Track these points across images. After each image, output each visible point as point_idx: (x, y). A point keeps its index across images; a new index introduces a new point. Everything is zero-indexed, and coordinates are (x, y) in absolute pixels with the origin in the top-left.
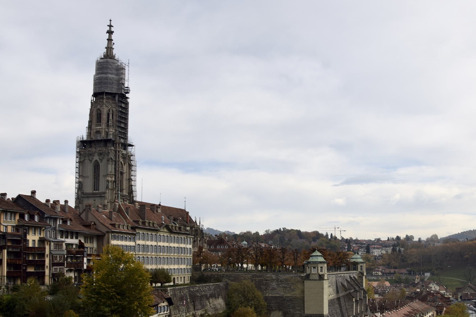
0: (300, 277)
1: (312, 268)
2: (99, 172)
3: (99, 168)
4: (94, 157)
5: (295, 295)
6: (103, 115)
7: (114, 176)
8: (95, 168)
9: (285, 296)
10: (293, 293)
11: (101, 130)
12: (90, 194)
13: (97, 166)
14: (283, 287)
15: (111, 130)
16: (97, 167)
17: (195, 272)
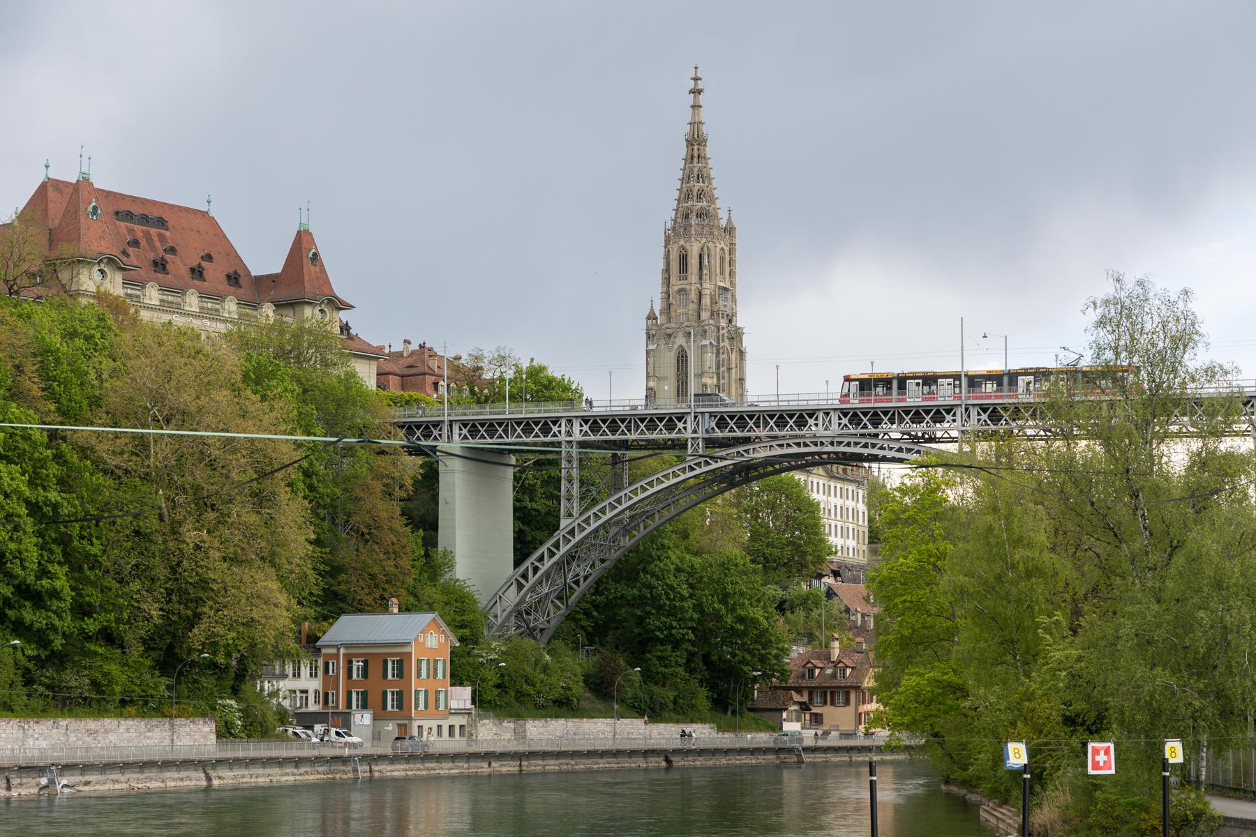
2: (687, 368)
3: (687, 360)
4: (677, 340)
6: (691, 258)
7: (715, 376)
8: (678, 361)
11: (688, 287)
13: (682, 356)
15: (708, 286)
17: (874, 558)
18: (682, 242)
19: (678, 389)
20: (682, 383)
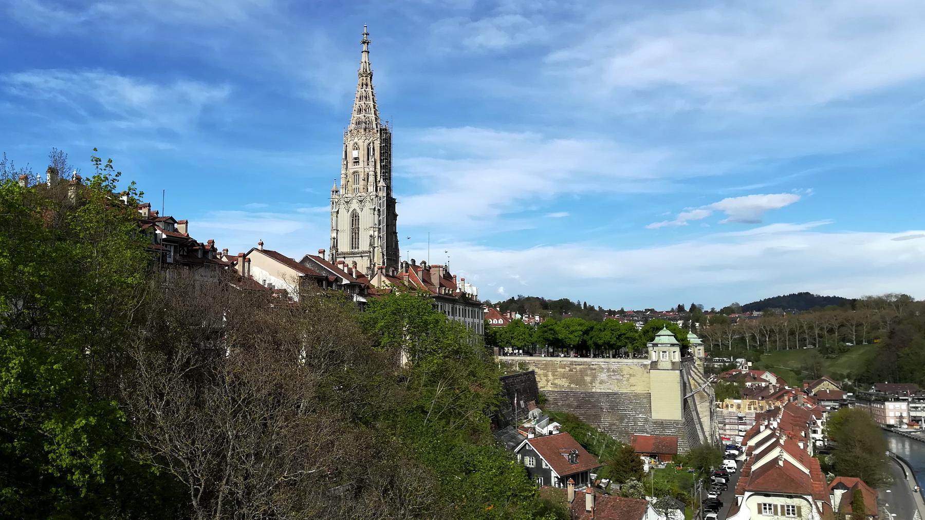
0: (642, 365)
1: (661, 352)
5: (635, 392)
8: (353, 220)
9: (621, 392)
10: (633, 388)
12: (347, 253)
13: (356, 217)
14: (617, 379)
16: (355, 217)
18: (356, 140)
19: (353, 239)
20: (355, 234)
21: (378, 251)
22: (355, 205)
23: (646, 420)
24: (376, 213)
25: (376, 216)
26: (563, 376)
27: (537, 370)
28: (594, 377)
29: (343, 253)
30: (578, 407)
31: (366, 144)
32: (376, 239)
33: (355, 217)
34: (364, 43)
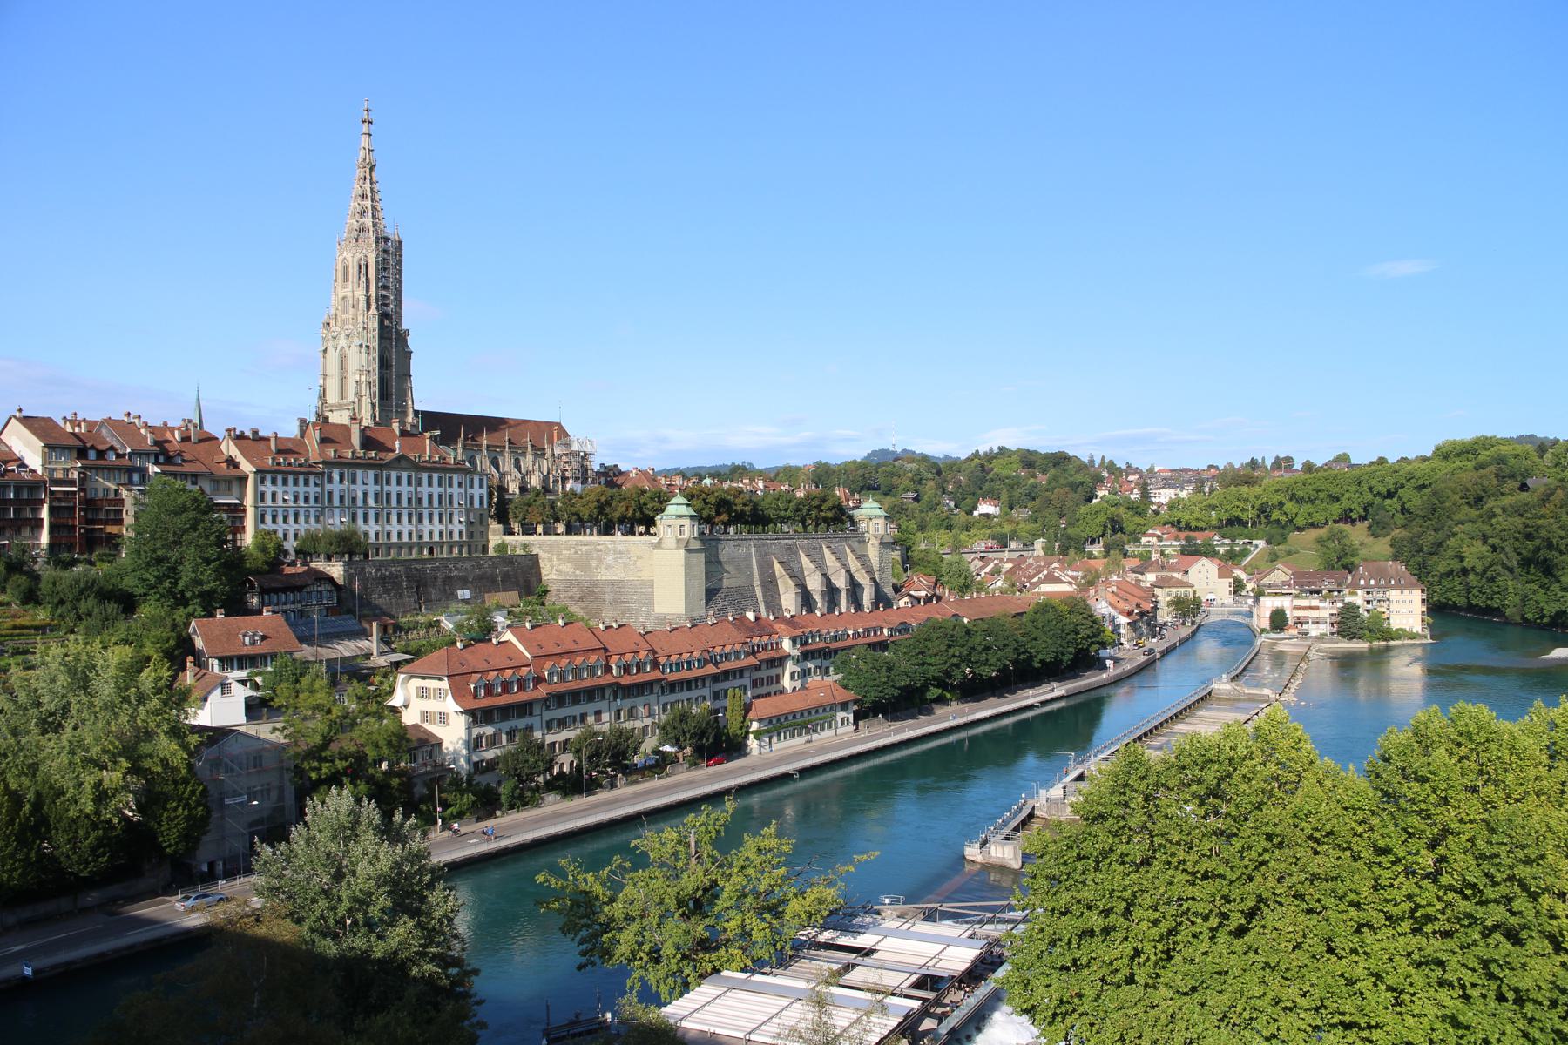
10: (639, 574)
16: (343, 359)
21: (366, 401)
22: (343, 342)
23: (648, 615)
24: (364, 350)
25: (365, 355)
26: (569, 560)
27: (543, 555)
28: (600, 560)
29: (332, 406)
30: (581, 599)
31: (356, 260)
32: (364, 385)
33: (343, 359)
34: (364, 122)
